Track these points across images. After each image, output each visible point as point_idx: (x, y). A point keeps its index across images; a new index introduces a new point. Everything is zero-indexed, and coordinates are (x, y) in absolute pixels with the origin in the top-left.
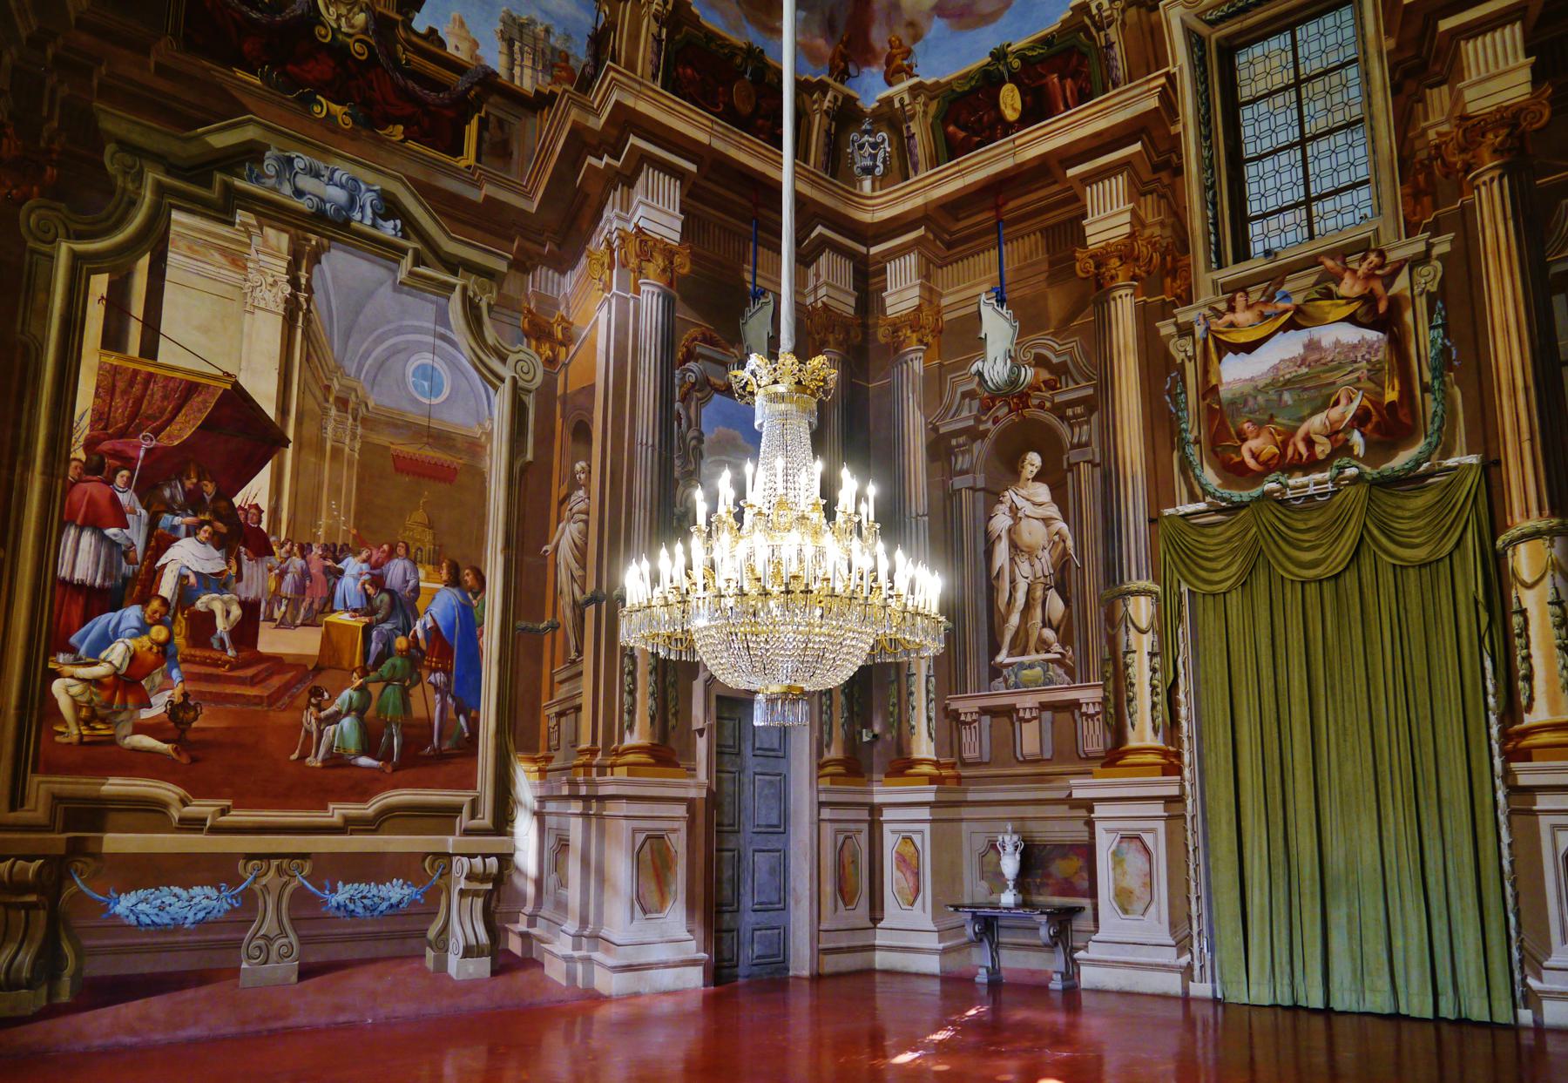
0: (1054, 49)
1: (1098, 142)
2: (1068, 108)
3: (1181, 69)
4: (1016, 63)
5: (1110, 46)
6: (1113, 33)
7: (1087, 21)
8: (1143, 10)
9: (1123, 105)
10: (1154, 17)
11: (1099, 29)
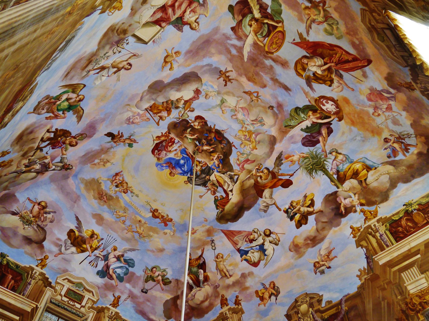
0: (17, 270)
1: (8, 306)
2: (7, 288)
3: (41, 307)
4: (5, 262)
5: (30, 284)
6: (33, 282)
7: (30, 273)
8: (43, 284)
9: (22, 303)
10: (44, 288)
11: (31, 277)
